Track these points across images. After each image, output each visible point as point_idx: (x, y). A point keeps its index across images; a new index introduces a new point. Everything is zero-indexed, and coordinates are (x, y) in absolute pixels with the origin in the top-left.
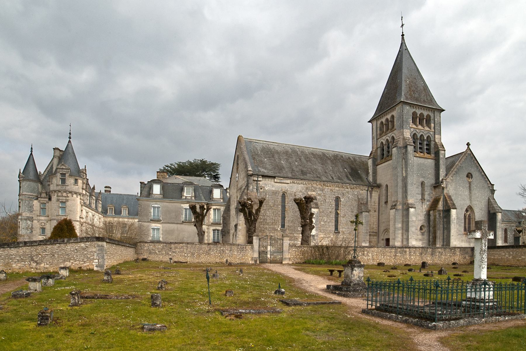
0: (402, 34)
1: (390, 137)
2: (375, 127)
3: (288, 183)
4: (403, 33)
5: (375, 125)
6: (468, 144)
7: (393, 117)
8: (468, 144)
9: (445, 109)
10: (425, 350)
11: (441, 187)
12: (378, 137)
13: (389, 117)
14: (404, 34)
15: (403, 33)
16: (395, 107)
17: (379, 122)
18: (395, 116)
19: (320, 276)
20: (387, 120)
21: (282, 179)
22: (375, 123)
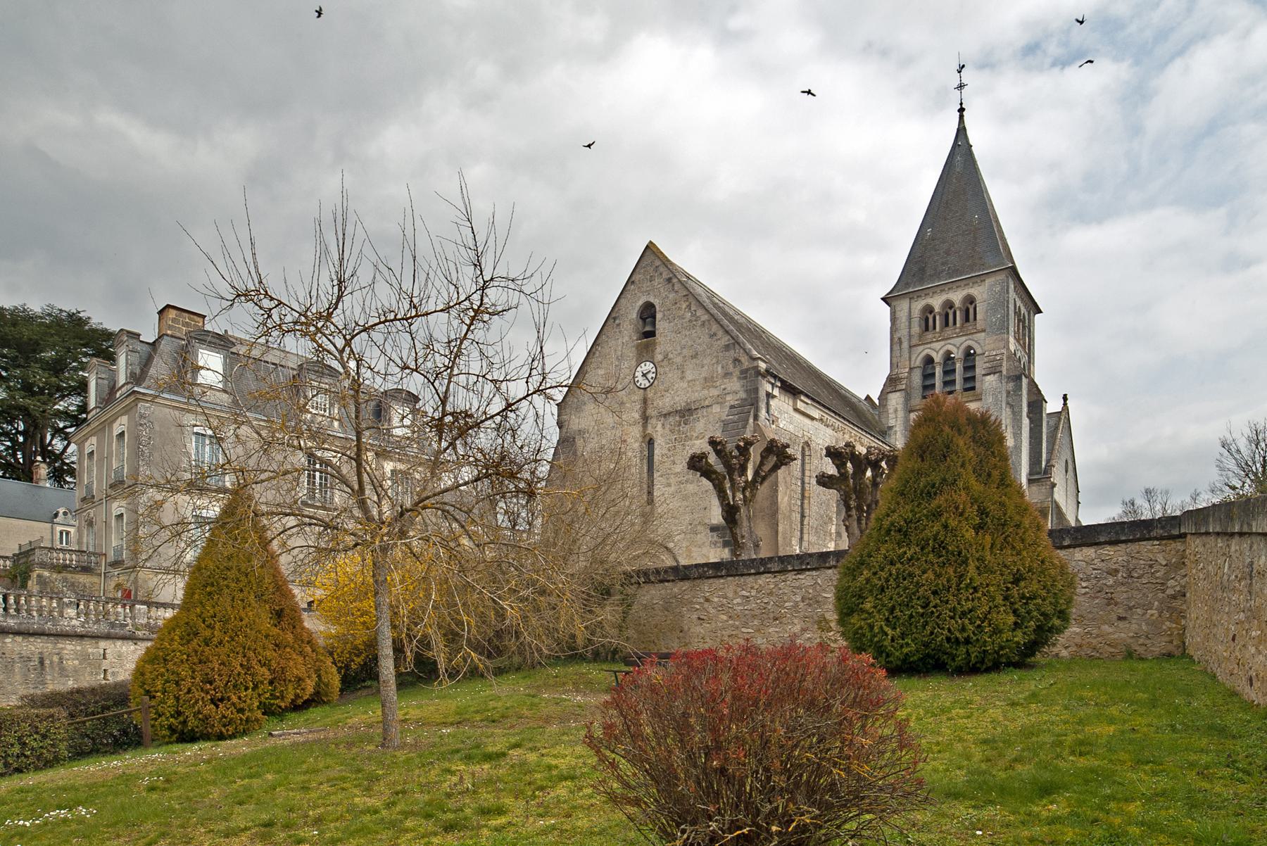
0: (959, 107)
1: (958, 348)
2: (906, 314)
3: (812, 419)
4: (961, 104)
5: (1013, 308)
6: (1065, 398)
7: (970, 300)
8: (1065, 398)
9: (1042, 310)
10: (647, 845)
11: (1049, 483)
12: (914, 341)
13: (957, 297)
14: (963, 106)
15: (961, 104)
16: (982, 278)
17: (918, 305)
18: (979, 298)
19: (982, 673)
20: (949, 305)
21: (809, 402)
22: (903, 306)
